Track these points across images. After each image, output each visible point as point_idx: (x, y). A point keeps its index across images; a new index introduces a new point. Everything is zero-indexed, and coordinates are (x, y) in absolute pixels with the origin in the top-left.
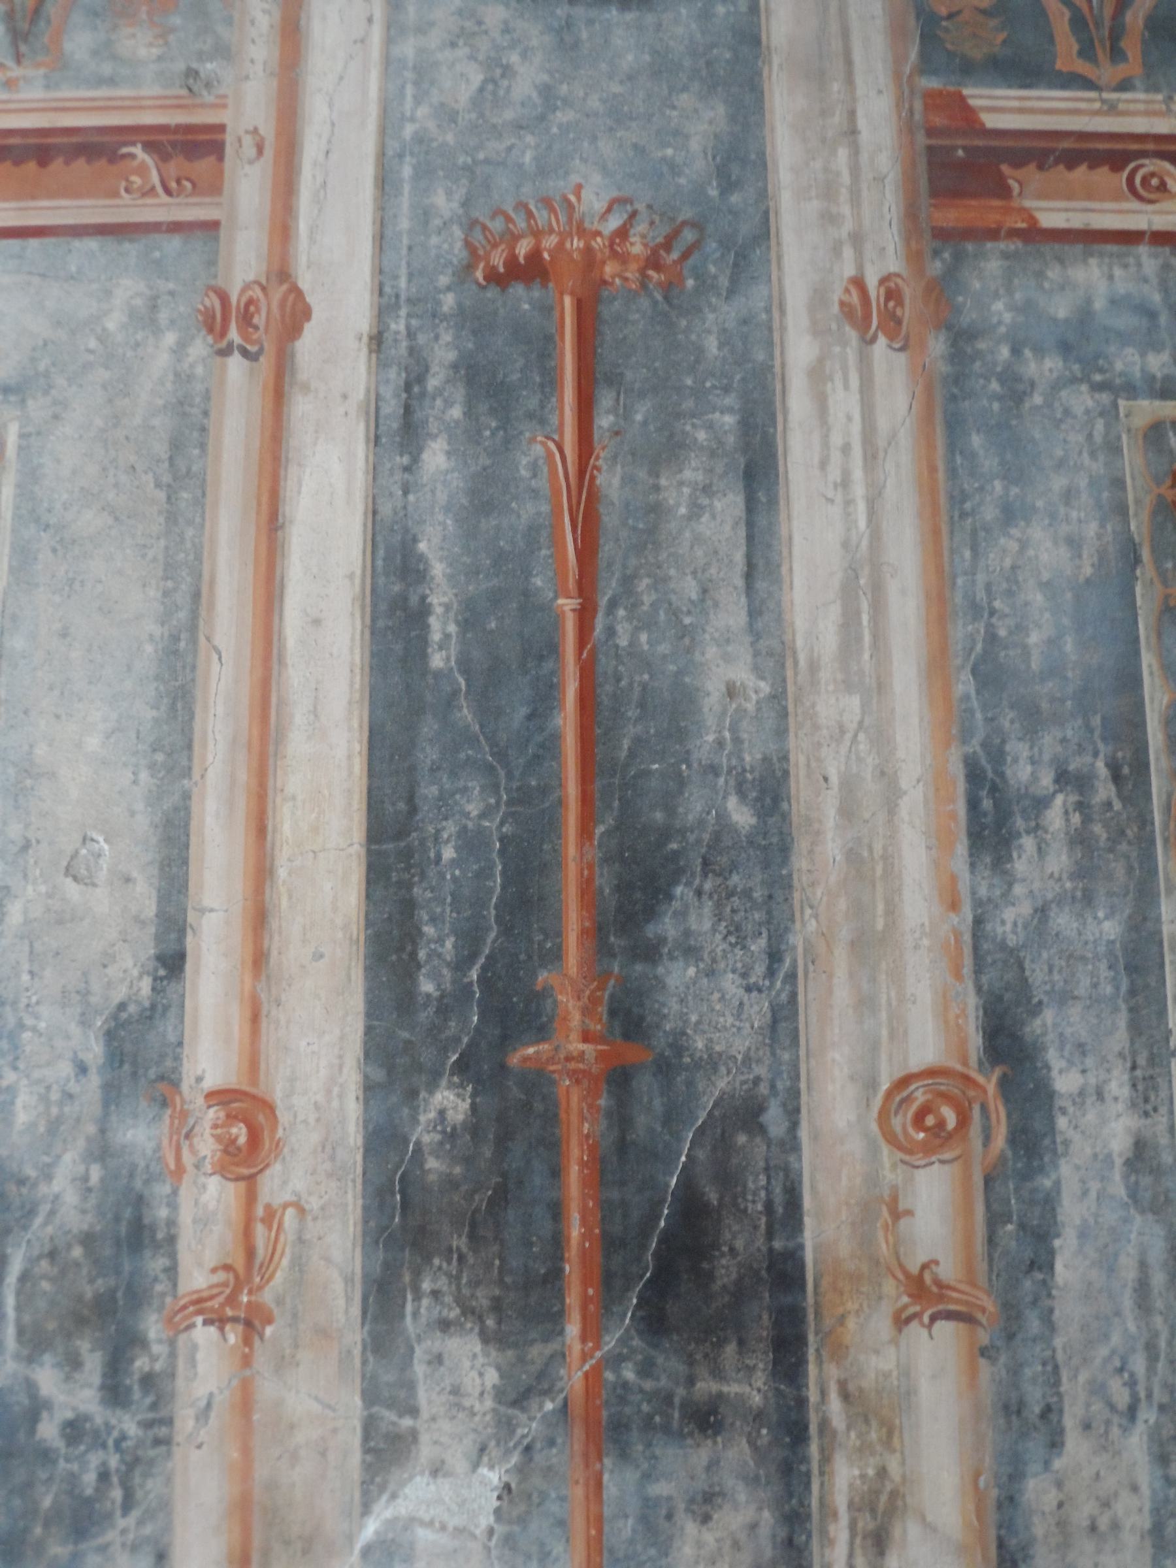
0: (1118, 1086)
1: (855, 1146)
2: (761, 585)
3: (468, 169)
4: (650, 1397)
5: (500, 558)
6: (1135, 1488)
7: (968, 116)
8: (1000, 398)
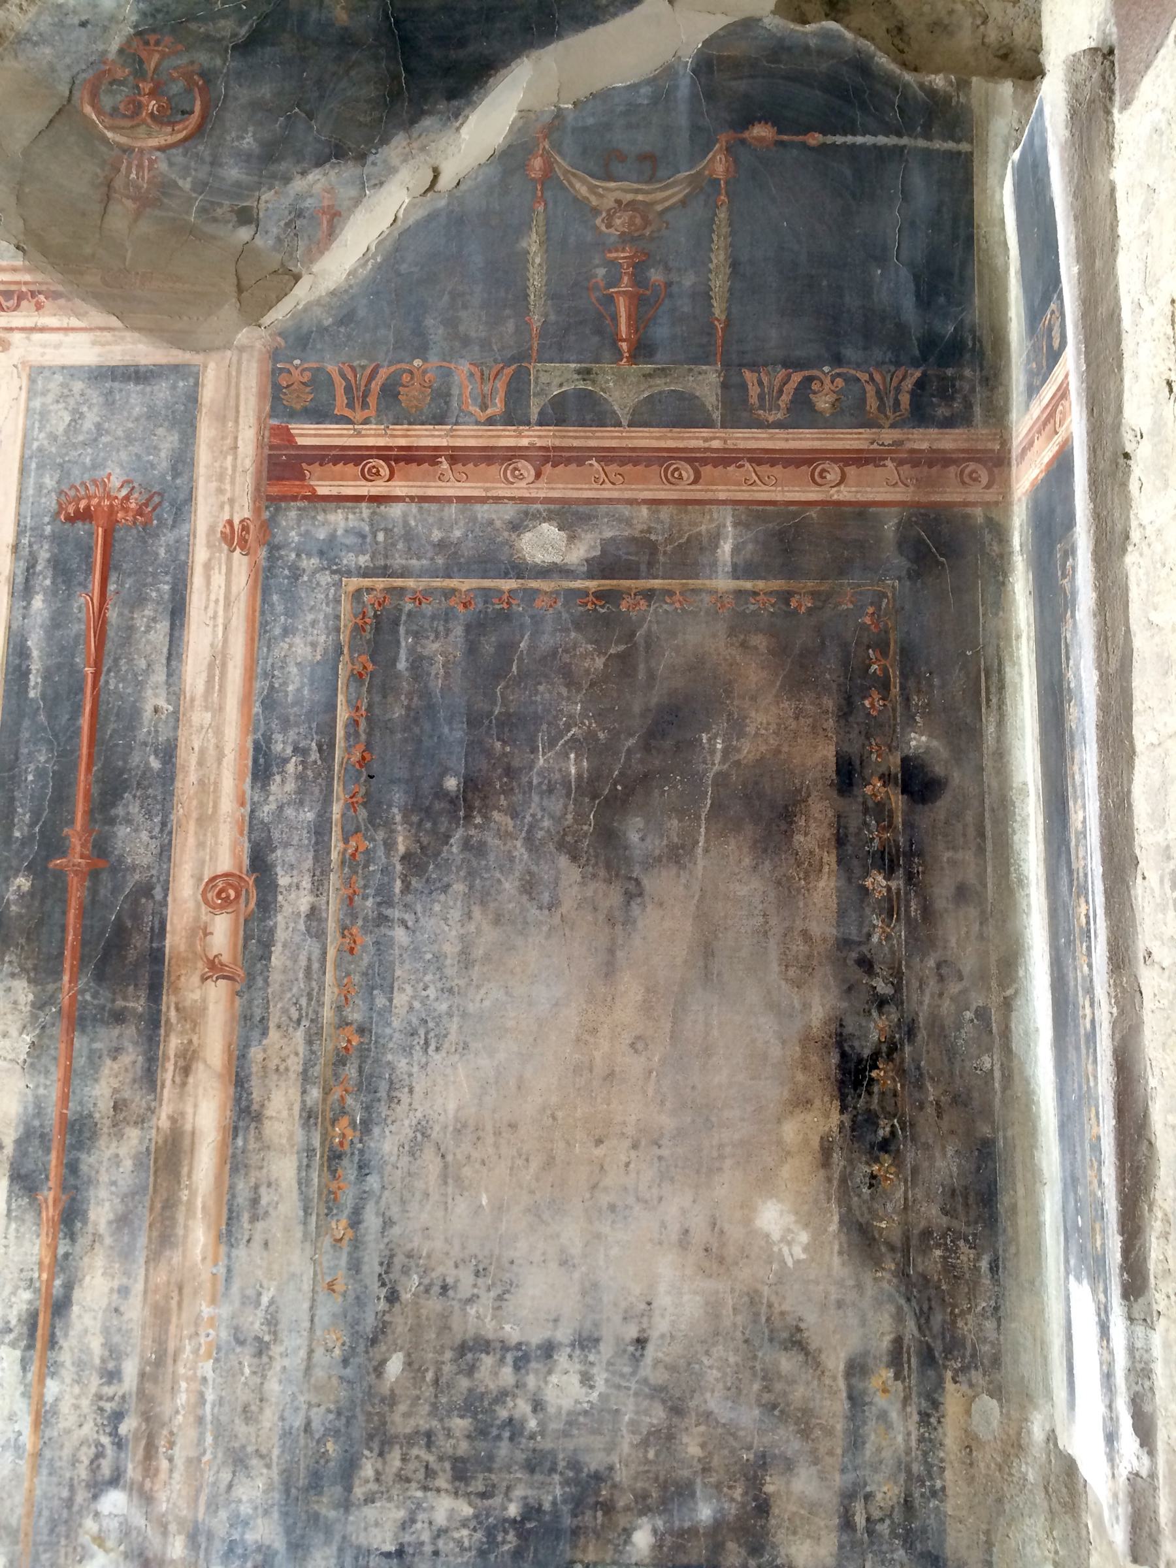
0: (306, 883)
1: (191, 905)
2: (173, 663)
3: (61, 465)
4: (96, 1007)
5: (62, 649)
6: (297, 1054)
7: (290, 438)
8: (288, 577)
